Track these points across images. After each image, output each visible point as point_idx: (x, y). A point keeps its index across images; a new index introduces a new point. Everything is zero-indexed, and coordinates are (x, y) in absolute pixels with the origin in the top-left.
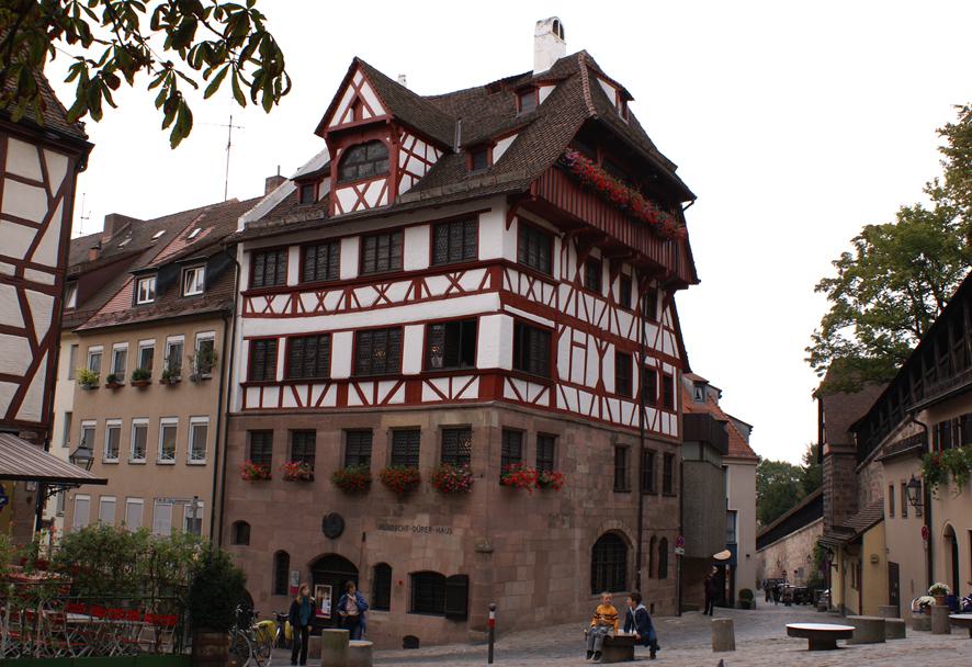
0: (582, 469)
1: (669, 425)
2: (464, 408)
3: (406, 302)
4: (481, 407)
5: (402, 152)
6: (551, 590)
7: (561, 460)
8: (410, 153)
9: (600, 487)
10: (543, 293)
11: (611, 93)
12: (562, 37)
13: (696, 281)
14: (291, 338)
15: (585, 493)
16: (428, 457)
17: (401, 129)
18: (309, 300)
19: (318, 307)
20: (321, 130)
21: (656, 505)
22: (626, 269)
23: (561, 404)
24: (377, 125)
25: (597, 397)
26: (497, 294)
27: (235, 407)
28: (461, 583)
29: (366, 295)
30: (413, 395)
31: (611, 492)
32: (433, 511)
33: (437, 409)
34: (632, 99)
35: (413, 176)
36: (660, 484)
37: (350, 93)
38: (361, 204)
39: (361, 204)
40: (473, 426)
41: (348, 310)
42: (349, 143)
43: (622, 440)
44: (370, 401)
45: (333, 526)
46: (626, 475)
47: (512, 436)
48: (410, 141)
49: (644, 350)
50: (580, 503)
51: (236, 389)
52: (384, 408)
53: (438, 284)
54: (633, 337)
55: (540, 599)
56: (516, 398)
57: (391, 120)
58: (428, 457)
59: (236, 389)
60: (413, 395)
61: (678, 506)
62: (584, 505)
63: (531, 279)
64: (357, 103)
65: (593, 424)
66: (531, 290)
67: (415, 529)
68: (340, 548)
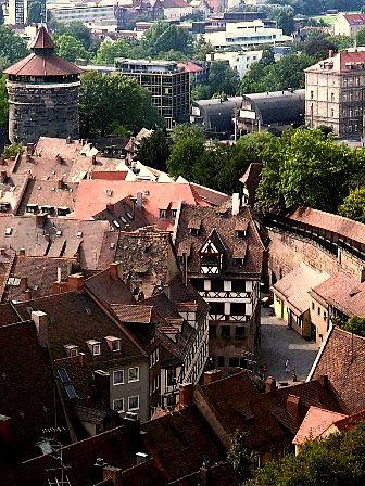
16: (232, 333)
53: (234, 295)
58: (232, 333)
64: (209, 247)
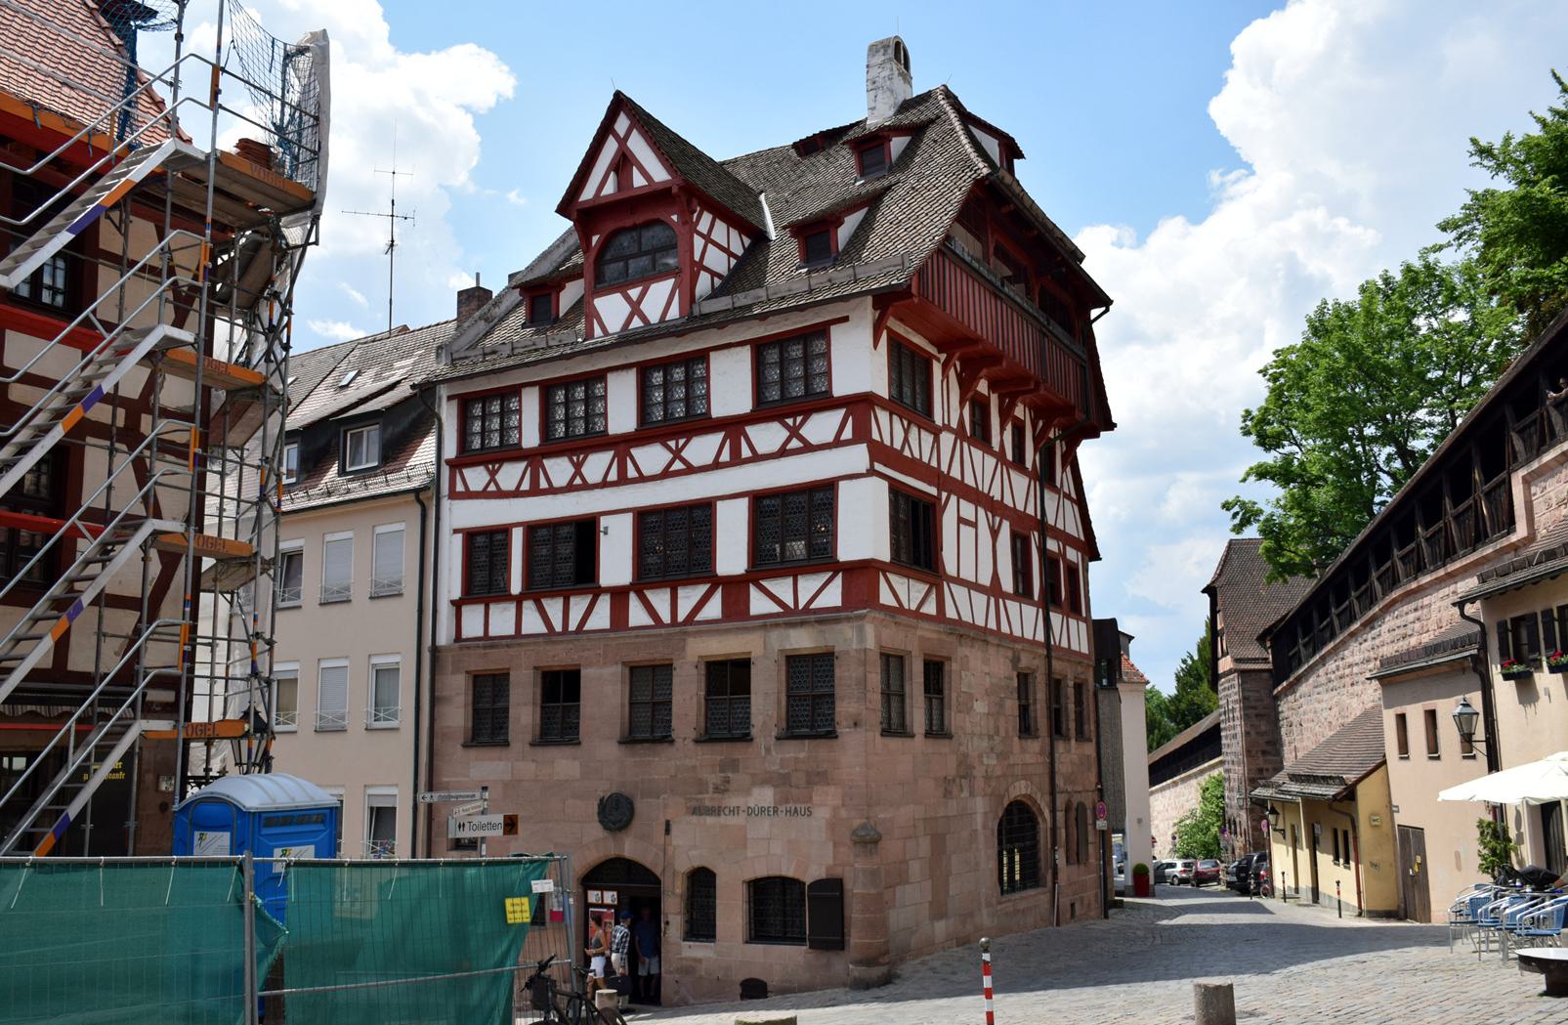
0: (981, 707)
1: (1076, 638)
2: (820, 622)
3: (717, 465)
4: (848, 619)
5: (696, 237)
6: (951, 893)
7: (954, 695)
8: (708, 239)
9: (1002, 733)
10: (920, 445)
11: (992, 146)
12: (907, 66)
13: (1111, 426)
14: (532, 529)
15: (985, 744)
17: (695, 201)
18: (559, 470)
19: (573, 478)
20: (563, 209)
21: (1072, 755)
22: (1019, 411)
23: (951, 613)
24: (657, 196)
25: (992, 600)
26: (864, 446)
27: (445, 637)
28: (831, 890)
29: (651, 457)
30: (736, 609)
31: (1016, 739)
32: (780, 781)
33: (777, 625)
34: (1020, 156)
35: (713, 274)
36: (1072, 725)
37: (611, 148)
38: (636, 318)
39: (636, 318)
40: (836, 649)
41: (623, 480)
42: (611, 226)
43: (1025, 661)
44: (666, 618)
45: (616, 812)
46: (1032, 714)
47: (893, 662)
48: (707, 217)
49: (1044, 528)
50: (980, 756)
51: (446, 612)
52: (690, 628)
53: (767, 436)
54: (1030, 511)
55: (939, 911)
56: (895, 604)
57: (680, 188)
59: (446, 612)
60: (736, 609)
61: (1094, 754)
62: (985, 760)
63: (905, 423)
65: (990, 639)
66: (906, 440)
67: (750, 811)
68: (630, 847)
